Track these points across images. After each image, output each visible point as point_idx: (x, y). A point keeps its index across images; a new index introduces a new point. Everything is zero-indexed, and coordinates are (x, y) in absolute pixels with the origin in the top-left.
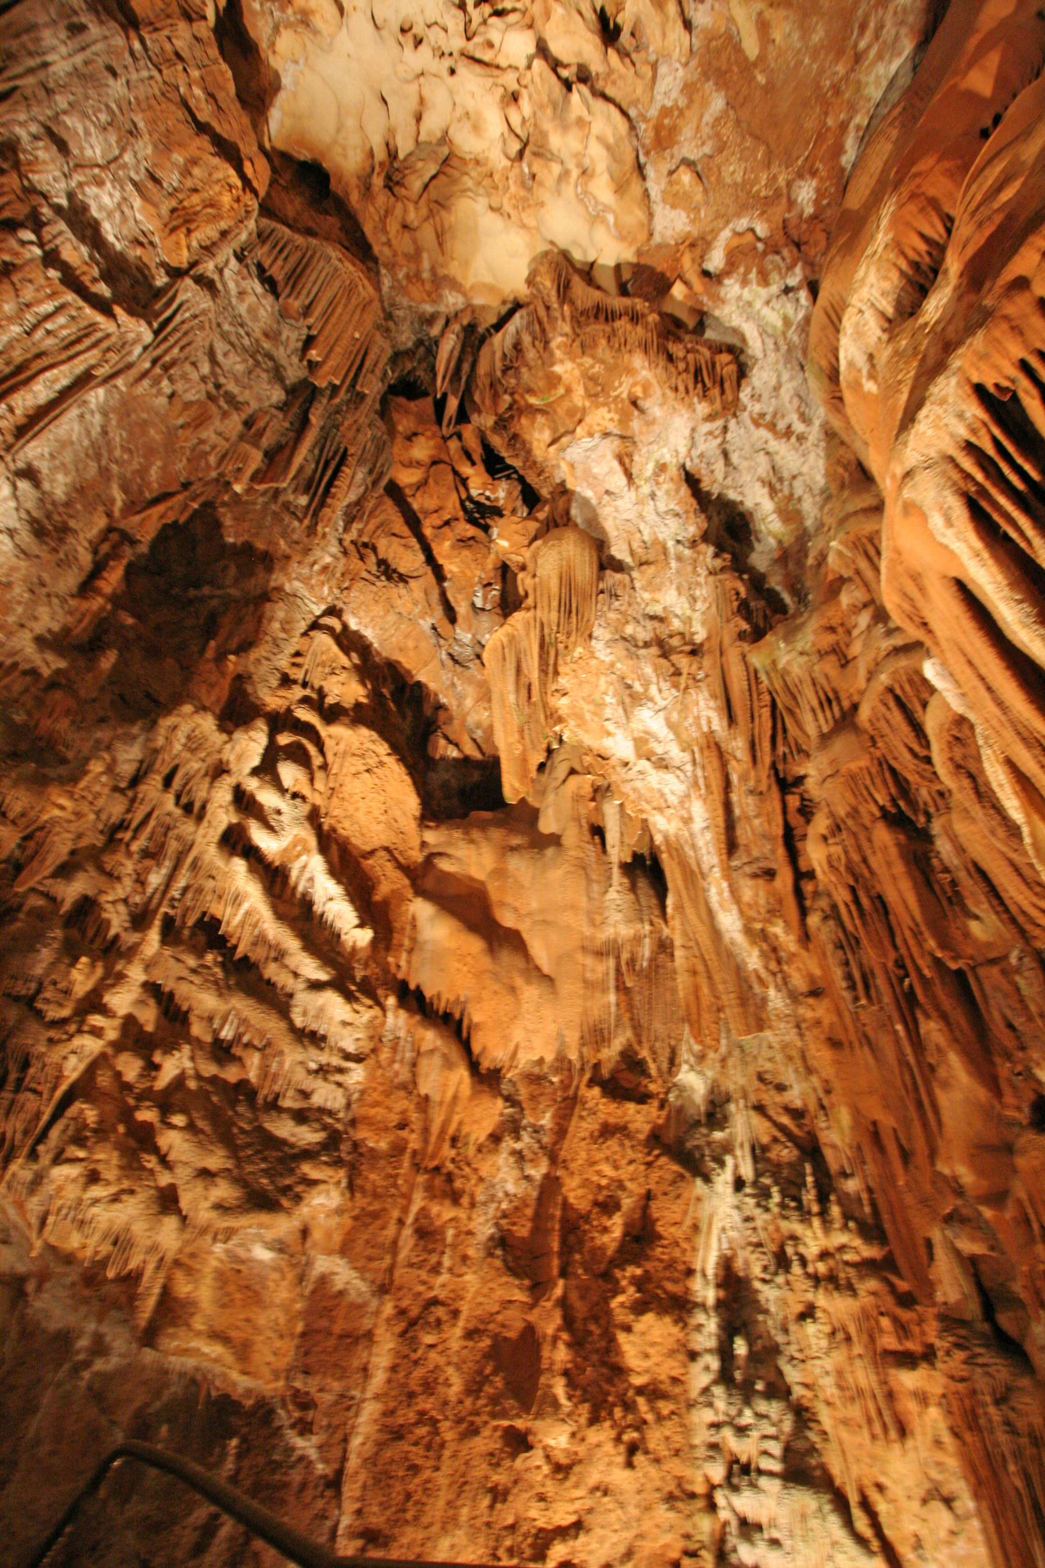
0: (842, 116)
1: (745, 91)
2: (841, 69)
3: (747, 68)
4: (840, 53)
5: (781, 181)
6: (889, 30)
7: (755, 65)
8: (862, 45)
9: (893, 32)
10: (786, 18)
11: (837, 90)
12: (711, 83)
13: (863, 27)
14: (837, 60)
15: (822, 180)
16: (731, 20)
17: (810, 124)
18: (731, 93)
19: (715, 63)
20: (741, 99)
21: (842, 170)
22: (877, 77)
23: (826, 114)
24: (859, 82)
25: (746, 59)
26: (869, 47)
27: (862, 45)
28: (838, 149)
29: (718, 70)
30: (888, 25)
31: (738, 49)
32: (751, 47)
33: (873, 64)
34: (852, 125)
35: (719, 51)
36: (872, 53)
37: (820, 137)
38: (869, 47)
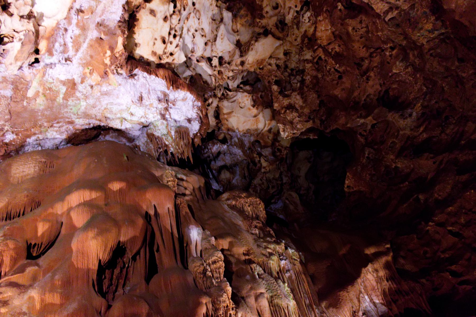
0: (37, 132)
1: (18, 100)
2: (45, 124)
3: (24, 97)
4: (48, 122)
5: (6, 128)
6: (63, 129)
7: (27, 98)
8: (55, 125)
9: (64, 130)
10: (43, 101)
11: (40, 126)
12: (12, 87)
13: (58, 123)
14: (46, 122)
15: (18, 138)
16: (31, 81)
17: (27, 125)
18: (14, 95)
19: (18, 84)
20: (15, 100)
21: (26, 141)
22: (52, 134)
23: (33, 128)
24: (47, 130)
25: (26, 94)
26: (56, 127)
27: (55, 125)
28: (29, 137)
29: (17, 86)
30: (64, 128)
31: (27, 89)
32: (30, 94)
33: (54, 131)
34: (37, 135)
35: (22, 83)
36: (55, 129)
37: (27, 130)
38: (56, 127)
